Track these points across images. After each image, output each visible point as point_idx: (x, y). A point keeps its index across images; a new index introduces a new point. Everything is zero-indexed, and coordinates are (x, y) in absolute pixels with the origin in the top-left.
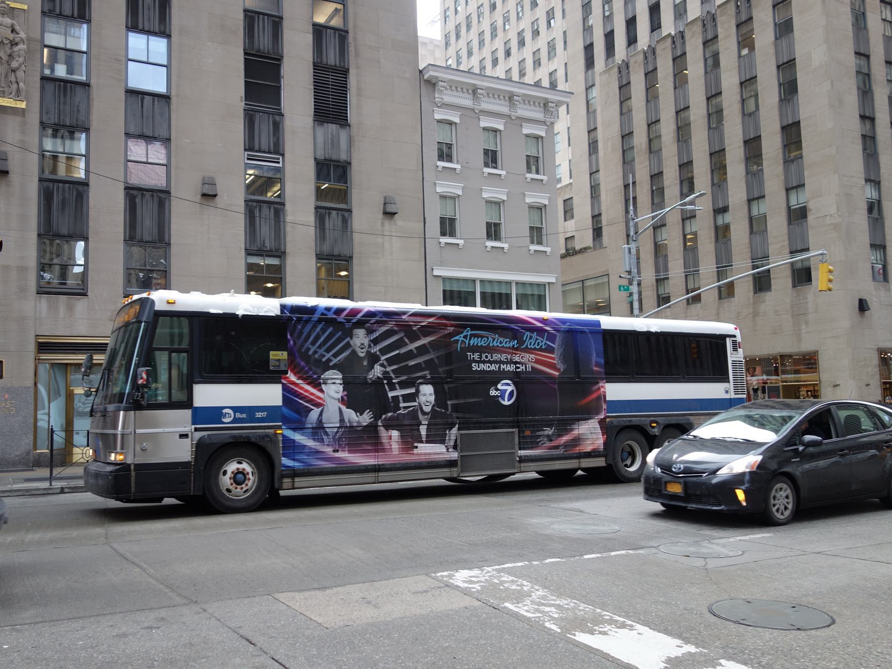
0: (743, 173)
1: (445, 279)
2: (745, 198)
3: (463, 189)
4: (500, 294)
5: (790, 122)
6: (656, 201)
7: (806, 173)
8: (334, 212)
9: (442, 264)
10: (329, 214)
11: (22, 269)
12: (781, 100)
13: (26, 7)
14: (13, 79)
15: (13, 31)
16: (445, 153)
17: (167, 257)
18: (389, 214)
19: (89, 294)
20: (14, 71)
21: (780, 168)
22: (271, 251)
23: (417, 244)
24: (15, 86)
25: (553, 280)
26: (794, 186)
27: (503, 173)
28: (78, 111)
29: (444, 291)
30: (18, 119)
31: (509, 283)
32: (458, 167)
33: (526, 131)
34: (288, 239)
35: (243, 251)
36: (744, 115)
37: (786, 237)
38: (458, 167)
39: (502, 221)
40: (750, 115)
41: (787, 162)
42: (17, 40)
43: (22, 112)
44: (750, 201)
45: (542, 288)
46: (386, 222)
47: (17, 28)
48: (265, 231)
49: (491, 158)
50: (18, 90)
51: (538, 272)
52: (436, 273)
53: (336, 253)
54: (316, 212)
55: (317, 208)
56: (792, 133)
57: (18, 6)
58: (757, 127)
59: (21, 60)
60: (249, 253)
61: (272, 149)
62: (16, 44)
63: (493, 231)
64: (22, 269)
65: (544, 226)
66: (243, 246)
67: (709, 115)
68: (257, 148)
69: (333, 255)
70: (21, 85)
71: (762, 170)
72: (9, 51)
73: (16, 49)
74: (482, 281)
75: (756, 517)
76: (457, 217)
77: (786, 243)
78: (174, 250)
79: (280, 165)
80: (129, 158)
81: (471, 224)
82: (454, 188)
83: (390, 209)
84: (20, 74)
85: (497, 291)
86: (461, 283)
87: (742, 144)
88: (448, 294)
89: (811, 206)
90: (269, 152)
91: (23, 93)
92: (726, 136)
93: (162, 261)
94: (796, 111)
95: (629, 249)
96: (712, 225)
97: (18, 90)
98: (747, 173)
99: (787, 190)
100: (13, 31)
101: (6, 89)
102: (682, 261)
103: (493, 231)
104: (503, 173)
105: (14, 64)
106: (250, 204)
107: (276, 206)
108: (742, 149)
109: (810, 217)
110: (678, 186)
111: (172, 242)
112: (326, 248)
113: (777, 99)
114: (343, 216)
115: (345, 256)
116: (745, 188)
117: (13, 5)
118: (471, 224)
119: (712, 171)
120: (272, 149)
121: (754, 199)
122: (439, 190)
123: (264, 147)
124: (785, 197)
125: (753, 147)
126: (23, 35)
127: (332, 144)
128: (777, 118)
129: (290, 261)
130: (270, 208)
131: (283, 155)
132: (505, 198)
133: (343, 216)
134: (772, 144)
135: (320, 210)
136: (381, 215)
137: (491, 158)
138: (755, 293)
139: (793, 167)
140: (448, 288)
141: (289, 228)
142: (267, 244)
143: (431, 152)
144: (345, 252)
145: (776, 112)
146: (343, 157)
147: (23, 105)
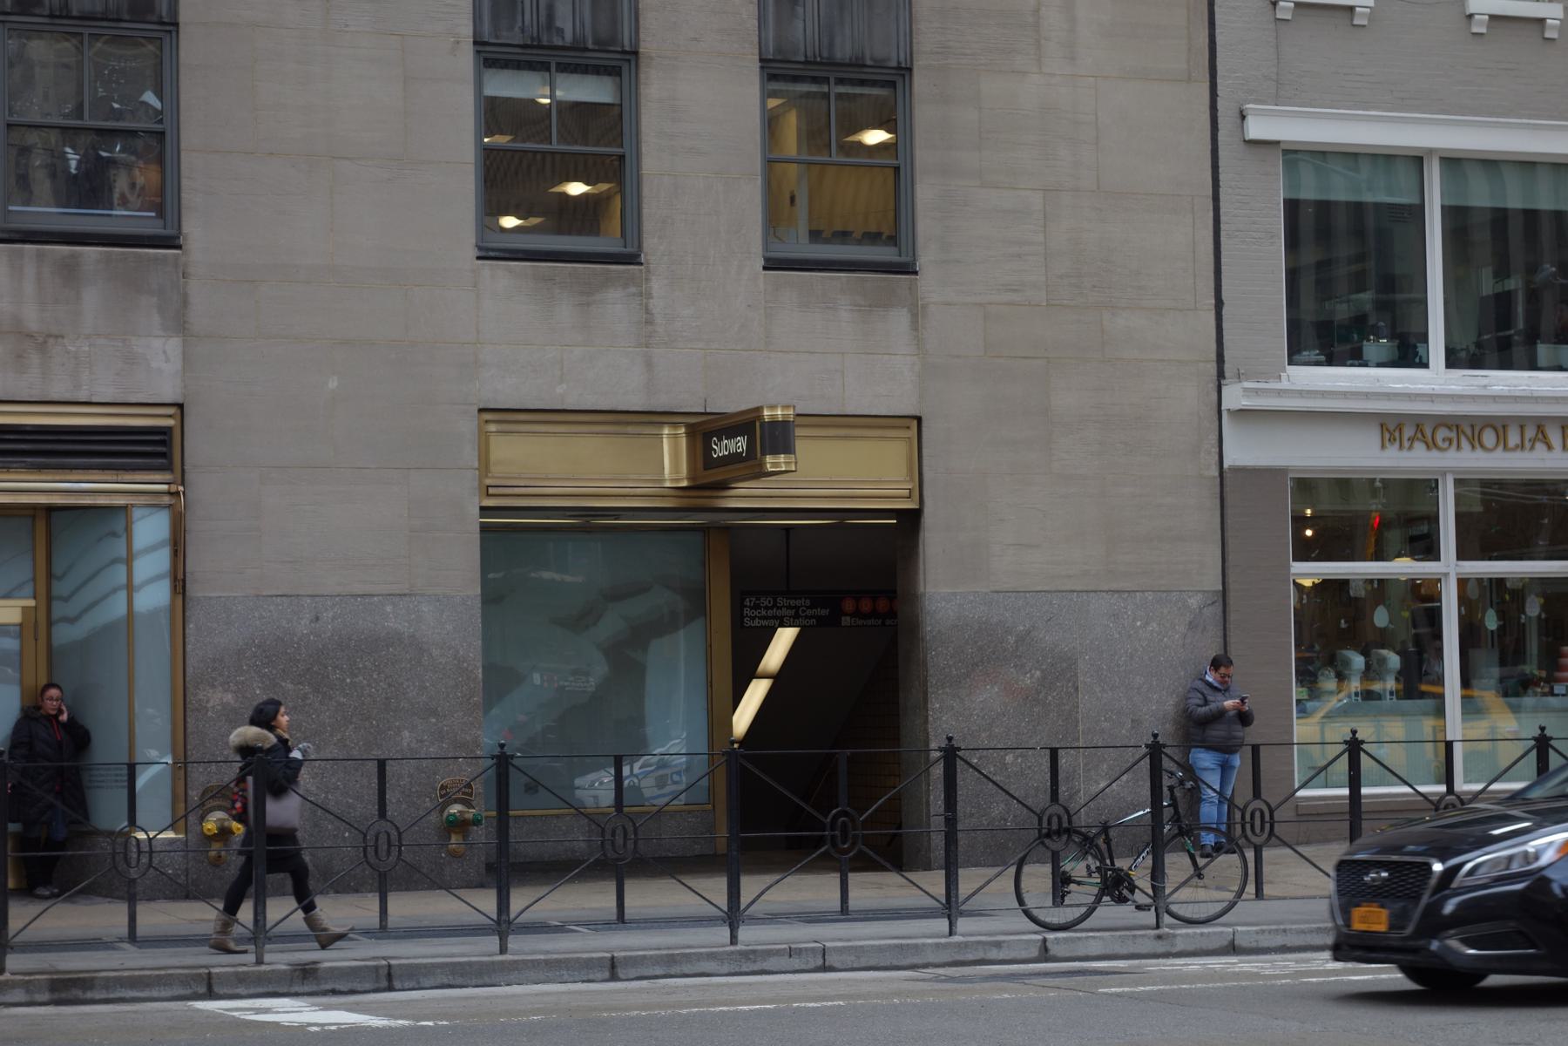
1: (1293, 155)
4: (1531, 216)
9: (1281, 93)
17: (164, 77)
22: (578, 47)
29: (1292, 207)
52: (1257, 129)
53: (843, 51)
60: (490, 56)
66: (467, 30)
69: (832, 63)
74: (1453, 163)
78: (193, 47)
93: (150, 97)
111: (183, 17)
112: (803, 34)
115: (879, 65)
129: (655, 88)
140: (1308, 193)
142: (564, 20)
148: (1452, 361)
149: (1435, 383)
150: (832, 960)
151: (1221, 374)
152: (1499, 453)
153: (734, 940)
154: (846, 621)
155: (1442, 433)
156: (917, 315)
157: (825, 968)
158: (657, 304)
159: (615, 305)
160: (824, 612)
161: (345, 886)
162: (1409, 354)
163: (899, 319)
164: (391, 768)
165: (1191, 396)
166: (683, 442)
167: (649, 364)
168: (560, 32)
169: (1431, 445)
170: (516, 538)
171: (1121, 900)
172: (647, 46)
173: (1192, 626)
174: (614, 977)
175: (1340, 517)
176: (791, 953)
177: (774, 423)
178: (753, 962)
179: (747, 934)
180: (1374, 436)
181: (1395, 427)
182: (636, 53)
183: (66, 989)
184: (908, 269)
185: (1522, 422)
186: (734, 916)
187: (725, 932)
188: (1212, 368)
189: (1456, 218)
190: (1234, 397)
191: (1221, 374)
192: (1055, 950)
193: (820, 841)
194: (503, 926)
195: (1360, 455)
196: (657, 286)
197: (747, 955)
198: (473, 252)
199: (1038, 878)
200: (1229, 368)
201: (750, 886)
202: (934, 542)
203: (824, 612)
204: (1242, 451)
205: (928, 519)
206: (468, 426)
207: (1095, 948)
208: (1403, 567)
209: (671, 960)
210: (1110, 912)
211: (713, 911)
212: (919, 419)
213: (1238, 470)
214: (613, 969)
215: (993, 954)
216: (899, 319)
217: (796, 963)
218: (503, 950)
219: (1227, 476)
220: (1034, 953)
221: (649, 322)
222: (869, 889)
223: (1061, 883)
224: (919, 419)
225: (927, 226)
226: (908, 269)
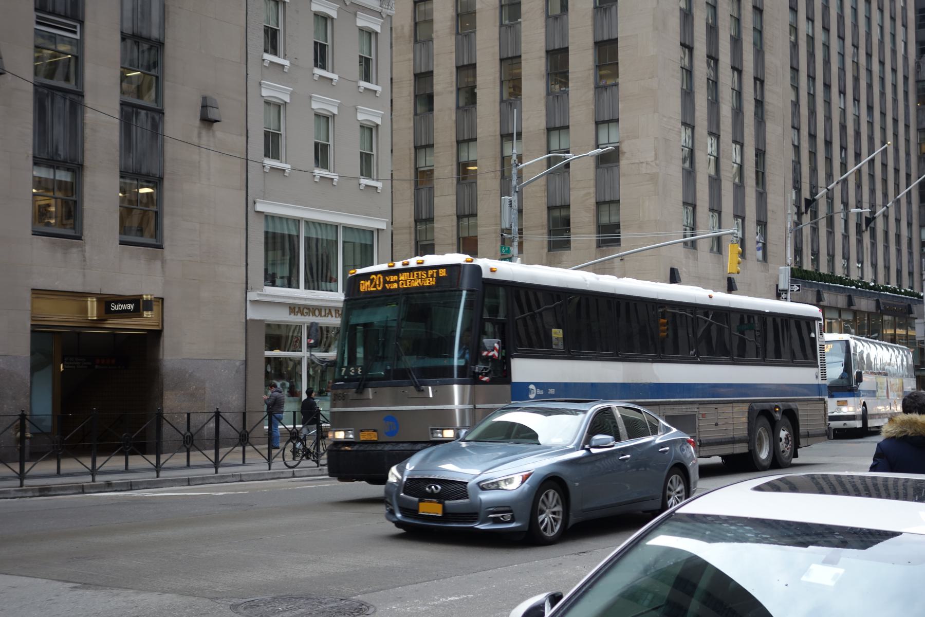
0: (543, 92)
1: (268, 217)
2: (543, 125)
3: (292, 94)
4: (283, 236)
5: (606, 38)
6: (419, 111)
7: (621, 106)
8: (143, 112)
9: (265, 196)
10: (137, 114)
12: (595, 8)
16: (272, 40)
18: (207, 121)
21: (590, 94)
22: (65, 162)
23: (238, 165)
25: (382, 226)
26: (606, 120)
27: (335, 77)
29: (266, 233)
31: (297, 221)
32: (286, 63)
33: (361, 23)
34: (87, 146)
35: (31, 159)
36: (548, 17)
37: (592, 183)
38: (286, 63)
39: (331, 142)
40: (556, 18)
41: (599, 88)
44: (549, 130)
45: (368, 236)
46: (204, 132)
48: (59, 131)
49: (321, 56)
51: (368, 214)
52: (259, 207)
53: (144, 171)
54: (122, 110)
55: (123, 104)
56: (607, 51)
58: (564, 35)
60: (37, 162)
61: (69, 12)
63: (321, 154)
65: (374, 152)
66: (31, 152)
67: (502, 6)
68: (50, 8)
69: (140, 174)
71: (567, 93)
74: (347, 228)
75: (529, 538)
76: (282, 132)
77: (593, 190)
79: (77, 37)
81: (299, 141)
82: (273, 90)
83: (212, 114)
85: (278, 231)
86: (277, 222)
87: (543, 54)
88: (270, 235)
89: (624, 147)
90: (66, 17)
92: (523, 39)
94: (613, 25)
95: (510, 201)
96: (499, 155)
98: (549, 93)
99: (597, 123)
102: (454, 197)
103: (321, 154)
104: (335, 77)
106: (40, 90)
107: (72, 96)
108: (544, 61)
109: (623, 162)
110: (454, 95)
113: (592, 6)
114: (153, 119)
115: (154, 176)
116: (544, 112)
118: (299, 141)
119: (502, 83)
120: (69, 12)
121: (555, 129)
122: (265, 93)
123: (60, 8)
124: (594, 132)
125: (557, 60)
127: (142, 13)
128: (590, 29)
130: (65, 99)
131: (82, 23)
132: (287, 99)
133: (153, 119)
134: (582, 62)
135: (126, 108)
136: (197, 122)
137: (321, 56)
138: (549, 250)
139: (606, 95)
140: (271, 230)
141: (87, 131)
143: (258, 39)
144: (155, 171)
145: (588, 22)
146: (155, 34)
148: (307, 287)
149: (301, 294)
150: (243, 478)
151: (247, 288)
152: (319, 318)
153: (216, 472)
154: (97, 367)
155: (305, 311)
156: (163, 262)
157: (241, 481)
158: (87, 255)
159: (74, 253)
160: (89, 363)
161: (173, 451)
162: (291, 282)
163: (158, 264)
164: (192, 416)
165: (239, 294)
166: (95, 304)
167: (84, 276)
168: (60, 156)
169: (302, 314)
170: (42, 335)
171: (308, 458)
172: (87, 163)
173: (237, 372)
174: (189, 485)
175: (276, 337)
176: (233, 476)
177: (147, 301)
178: (223, 479)
179: (163, 474)
180: (287, 311)
181: (294, 309)
182: (82, 165)
183: (44, 491)
184: (160, 247)
185: (325, 308)
186: (94, 472)
187: (213, 470)
188: (244, 286)
189: (308, 239)
190: (252, 296)
191: (247, 288)
192: (296, 474)
193: (119, 445)
194: (94, 472)
195: (282, 316)
196: (87, 248)
197: (222, 477)
198: (30, 232)
199: (288, 452)
200: (249, 285)
201: (100, 461)
202: (167, 341)
203: (89, 363)
204: (253, 314)
205: (166, 332)
206: (28, 295)
207: (305, 473)
208: (319, 355)
209: (203, 479)
210: (305, 463)
211: (152, 466)
212: (163, 299)
213: (251, 320)
214: (189, 482)
215: (282, 476)
216: (158, 264)
217: (234, 479)
218: (158, 476)
219: (249, 324)
220: (291, 475)
221: (85, 261)
222: (136, 461)
223: (295, 452)
224: (163, 299)
225: (167, 233)
226: (160, 247)
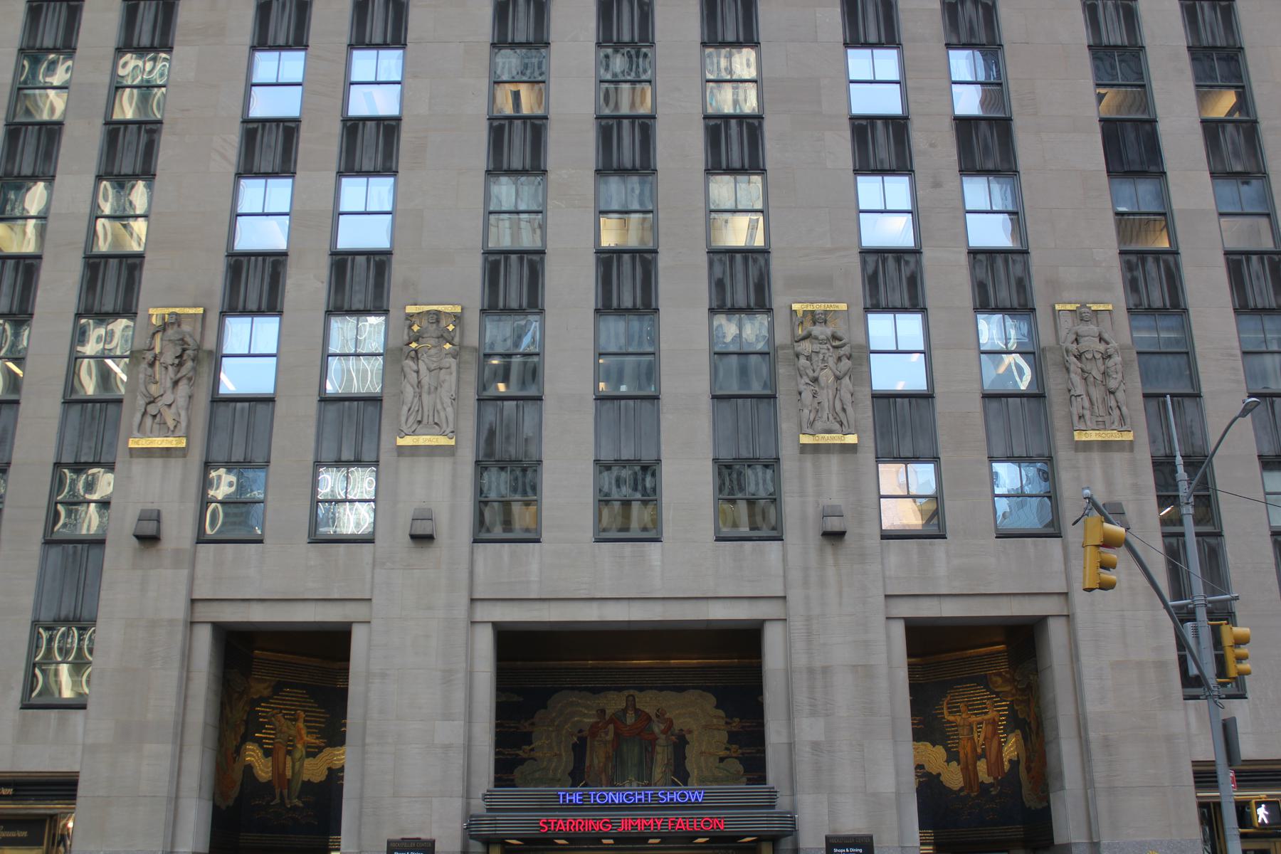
11: (1161, 665)
13: (1110, 307)
14: (1113, 403)
15: (1101, 339)
19: (1249, 695)
20: (1112, 393)
24: (1116, 413)
28: (1192, 433)
30: (1126, 455)
42: (1111, 351)
43: (1130, 446)
47: (1106, 336)
50: (1122, 417)
57: (1101, 307)
59: (1120, 376)
62: (1110, 356)
64: (1161, 665)
70: (1124, 409)
72: (1102, 368)
73: (1110, 363)
80: (1268, 490)
84: (1120, 395)
91: (1128, 421)
97: (1122, 417)
100: (1101, 339)
101: (1107, 418)
105: (1112, 384)
117: (1094, 307)
126: (1114, 344)
147: (1128, 437)
